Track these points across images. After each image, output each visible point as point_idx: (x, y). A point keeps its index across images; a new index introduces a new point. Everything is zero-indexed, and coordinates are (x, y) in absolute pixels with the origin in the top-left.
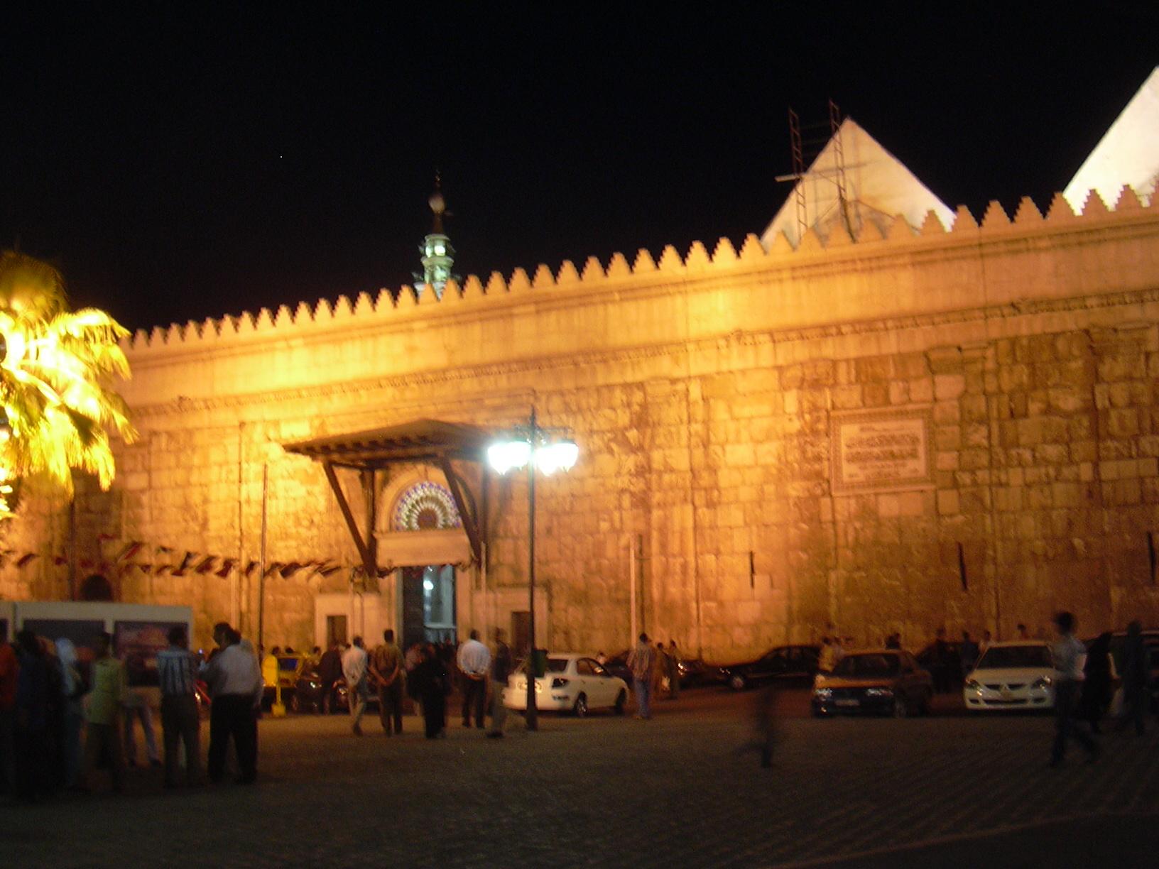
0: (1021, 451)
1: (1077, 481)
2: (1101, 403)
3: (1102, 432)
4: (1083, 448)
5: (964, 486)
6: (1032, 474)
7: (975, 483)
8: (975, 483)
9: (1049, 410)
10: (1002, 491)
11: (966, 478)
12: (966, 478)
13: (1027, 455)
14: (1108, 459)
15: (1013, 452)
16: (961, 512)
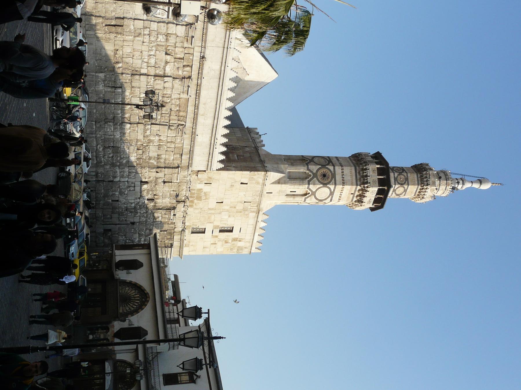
0: (154, 51)
1: (141, 68)
2: (166, 79)
3: (157, 78)
4: (152, 72)
5: (144, 31)
6: (145, 54)
7: (144, 35)
8: (144, 35)
9: (167, 63)
10: (141, 43)
11: (147, 32)
12: (147, 32)
13: (152, 53)
14: (148, 78)
15: (154, 48)
16: (135, 28)
